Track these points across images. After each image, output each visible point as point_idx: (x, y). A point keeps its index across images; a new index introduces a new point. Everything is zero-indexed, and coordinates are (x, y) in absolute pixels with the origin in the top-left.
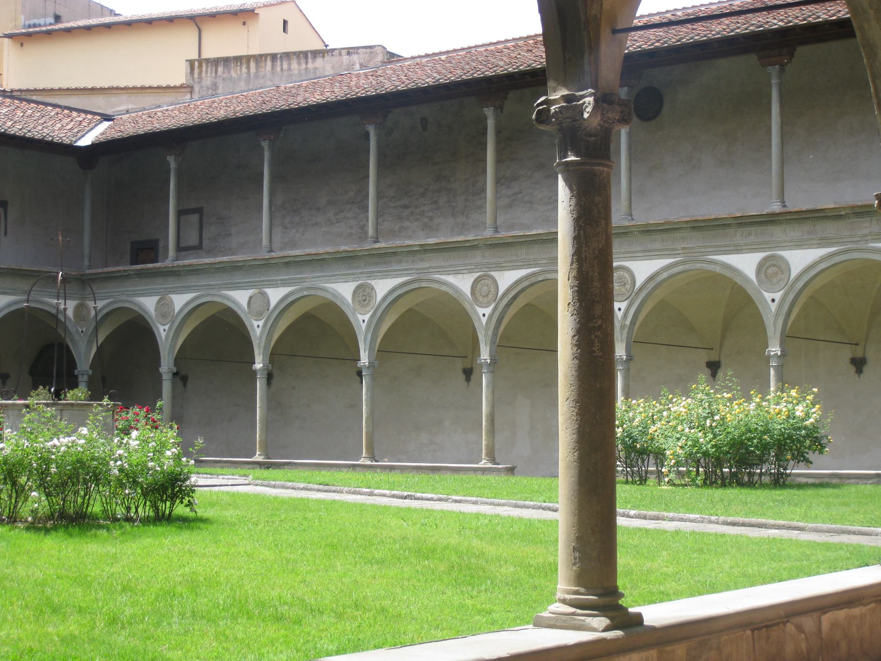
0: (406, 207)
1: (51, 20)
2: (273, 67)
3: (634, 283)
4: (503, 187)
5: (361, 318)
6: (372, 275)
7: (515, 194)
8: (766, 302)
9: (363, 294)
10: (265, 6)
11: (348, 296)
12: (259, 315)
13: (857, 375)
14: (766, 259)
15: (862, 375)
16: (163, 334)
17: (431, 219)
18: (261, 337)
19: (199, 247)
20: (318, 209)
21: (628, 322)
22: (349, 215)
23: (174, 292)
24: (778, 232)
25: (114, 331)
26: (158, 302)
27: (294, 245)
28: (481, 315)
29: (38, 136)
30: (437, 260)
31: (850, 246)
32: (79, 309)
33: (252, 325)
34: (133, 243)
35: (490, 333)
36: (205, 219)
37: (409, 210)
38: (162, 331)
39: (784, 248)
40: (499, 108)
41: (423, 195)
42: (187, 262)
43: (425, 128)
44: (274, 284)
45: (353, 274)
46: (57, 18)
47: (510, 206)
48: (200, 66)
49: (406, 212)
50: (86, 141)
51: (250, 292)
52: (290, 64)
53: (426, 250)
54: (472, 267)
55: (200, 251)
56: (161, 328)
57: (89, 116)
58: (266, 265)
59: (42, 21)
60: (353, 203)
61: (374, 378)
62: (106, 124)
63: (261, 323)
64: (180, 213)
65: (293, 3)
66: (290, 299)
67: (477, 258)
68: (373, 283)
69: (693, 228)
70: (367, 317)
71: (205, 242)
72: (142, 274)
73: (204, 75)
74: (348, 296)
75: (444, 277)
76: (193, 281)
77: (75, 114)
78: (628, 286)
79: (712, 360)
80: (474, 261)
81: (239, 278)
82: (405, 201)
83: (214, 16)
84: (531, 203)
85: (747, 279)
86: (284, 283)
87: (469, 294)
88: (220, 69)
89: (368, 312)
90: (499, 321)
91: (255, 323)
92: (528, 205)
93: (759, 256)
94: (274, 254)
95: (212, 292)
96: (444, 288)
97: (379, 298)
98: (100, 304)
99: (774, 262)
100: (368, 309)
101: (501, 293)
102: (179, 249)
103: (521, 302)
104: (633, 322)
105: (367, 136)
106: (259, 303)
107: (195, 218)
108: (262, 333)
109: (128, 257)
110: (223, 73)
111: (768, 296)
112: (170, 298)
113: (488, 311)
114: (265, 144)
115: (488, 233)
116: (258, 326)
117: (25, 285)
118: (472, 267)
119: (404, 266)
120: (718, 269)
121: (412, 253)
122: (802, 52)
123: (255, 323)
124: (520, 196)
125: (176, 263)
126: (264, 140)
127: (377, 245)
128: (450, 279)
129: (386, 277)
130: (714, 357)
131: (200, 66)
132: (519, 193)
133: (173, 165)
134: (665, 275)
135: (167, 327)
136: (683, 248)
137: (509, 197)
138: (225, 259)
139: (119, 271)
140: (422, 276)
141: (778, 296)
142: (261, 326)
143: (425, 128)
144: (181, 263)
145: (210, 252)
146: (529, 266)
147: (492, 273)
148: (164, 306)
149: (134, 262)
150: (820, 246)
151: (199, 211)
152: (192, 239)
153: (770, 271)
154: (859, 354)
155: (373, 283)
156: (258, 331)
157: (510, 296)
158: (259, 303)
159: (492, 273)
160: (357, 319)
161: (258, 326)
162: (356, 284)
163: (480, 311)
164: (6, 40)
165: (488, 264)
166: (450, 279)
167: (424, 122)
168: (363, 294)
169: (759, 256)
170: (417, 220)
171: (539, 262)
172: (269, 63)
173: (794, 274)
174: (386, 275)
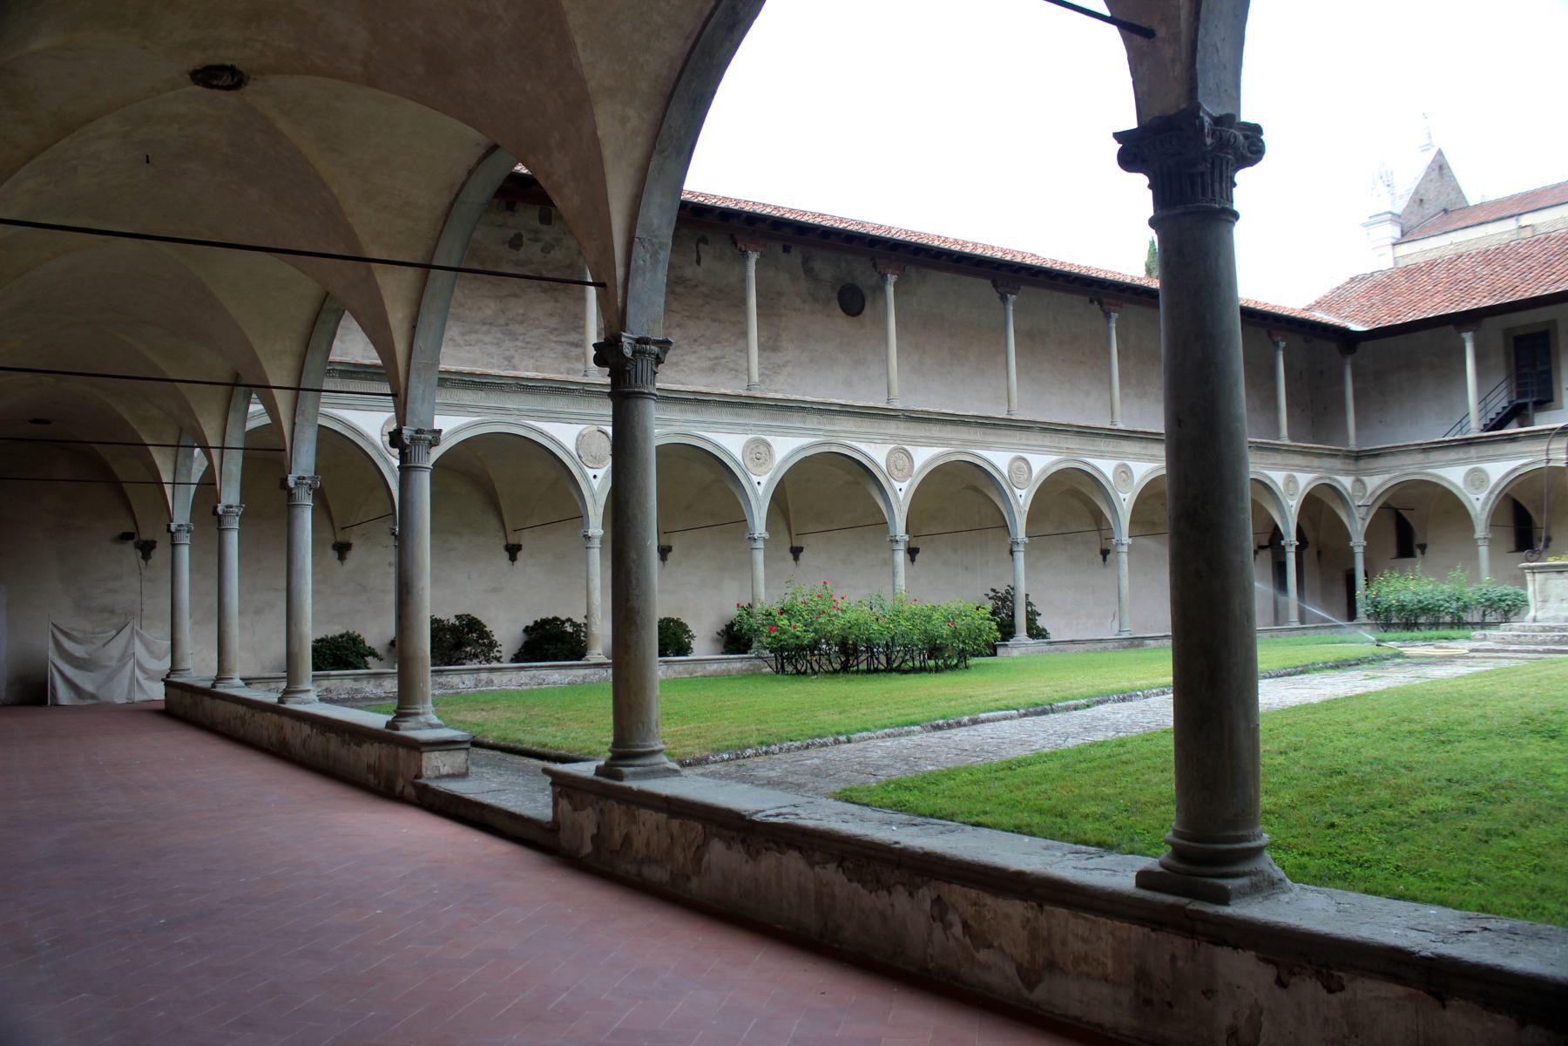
4: (703, 347)
7: (716, 358)
22: (487, 339)
28: (591, 477)
47: (713, 369)
54: (887, 437)
84: (737, 371)
89: (766, 473)
92: (734, 372)
100: (763, 469)
116: (595, 477)
118: (887, 437)
124: (724, 361)
128: (862, 446)
132: (723, 357)
137: (710, 359)
140: (834, 440)
142: (899, 492)
161: (595, 477)
168: (760, 451)
171: (953, 442)
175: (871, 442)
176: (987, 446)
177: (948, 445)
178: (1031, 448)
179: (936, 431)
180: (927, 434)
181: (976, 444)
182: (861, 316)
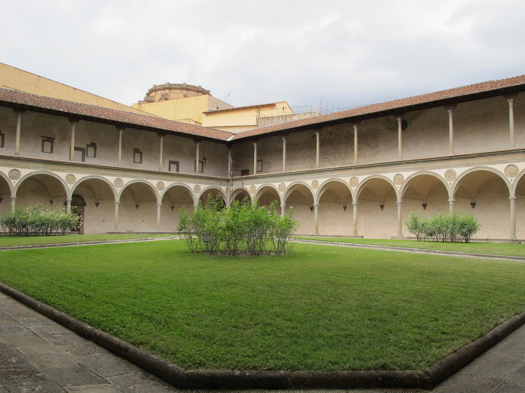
0: (325, 158)
1: (216, 109)
2: (282, 120)
3: (403, 179)
5: (314, 191)
6: (318, 177)
8: (448, 184)
9: (315, 183)
10: (278, 103)
11: (310, 185)
12: (282, 190)
13: (473, 208)
14: (448, 171)
15: (474, 208)
16: (253, 196)
17: (333, 161)
18: (283, 196)
19: (261, 171)
20: (298, 159)
21: (401, 191)
23: (256, 184)
24: (452, 162)
25: (237, 195)
26: (251, 186)
27: (291, 170)
29: (215, 138)
30: (339, 173)
31: (477, 166)
32: (227, 189)
33: (280, 193)
34: (242, 171)
35: (356, 195)
36: (263, 163)
37: (326, 159)
38: (253, 195)
39: (454, 167)
40: (358, 126)
41: (331, 154)
42: (260, 175)
43: (331, 135)
44: (287, 181)
45: (312, 177)
46: (218, 108)
48: (260, 120)
49: (325, 160)
50: (229, 139)
51: (279, 184)
52: (287, 118)
53: (335, 170)
55: (262, 172)
56: (252, 194)
57: (229, 134)
58: (285, 175)
59: (213, 109)
60: (309, 157)
61: (319, 208)
62: (234, 136)
63: (283, 192)
64: (258, 161)
65: (285, 103)
66: (292, 185)
67: (352, 172)
68: (318, 180)
69: (423, 161)
70: (316, 190)
71: (263, 170)
72: (246, 178)
73: (261, 122)
74: (310, 185)
75: (341, 178)
76: (262, 180)
77: (225, 133)
78: (401, 180)
79: (424, 204)
80: (351, 173)
81: (276, 179)
82: (325, 156)
83: (263, 106)
84: (365, 156)
85: (442, 178)
86: (290, 180)
87: (349, 183)
88: (266, 120)
90: (359, 191)
91: (281, 193)
93: (445, 170)
94: (287, 172)
95: (268, 183)
96: (341, 181)
97: (320, 184)
98: (234, 187)
99: (451, 172)
101: (359, 183)
102: (257, 172)
103: (365, 186)
104: (403, 191)
105: (314, 137)
106: (282, 186)
107: (260, 163)
108: (283, 195)
109: (240, 174)
110: (267, 121)
111: (449, 183)
112: (255, 186)
113: (355, 188)
114: (284, 139)
115: (355, 164)
117: (211, 182)
119: (328, 175)
120: (431, 174)
121: (330, 170)
122: (459, 105)
123: (281, 193)
125: (257, 175)
126: (284, 138)
127: (319, 169)
128: (343, 178)
129: (322, 178)
130: (425, 203)
131: (260, 120)
132: (361, 153)
133: (255, 146)
134: (414, 176)
135: (254, 194)
136: (420, 168)
138: (272, 173)
139: (239, 178)
140: (334, 178)
141: (452, 182)
143: (331, 135)
144: (258, 175)
145: (264, 173)
146: (369, 174)
147: (356, 176)
148: (253, 187)
149: (242, 174)
150: (467, 166)
151: (262, 161)
152: (260, 170)
153: (449, 174)
154: (473, 201)
155: (318, 180)
156: (282, 195)
157: (362, 183)
158: (282, 186)
159: (356, 176)
160: (313, 191)
162: (313, 180)
163: (353, 188)
164: (204, 114)
165: (355, 173)
166: (343, 178)
167: (331, 133)
168: (315, 183)
169: (445, 170)
170: (329, 162)
172: (281, 118)
173: (457, 176)
174: (322, 177)
175: (345, 177)
176: (385, 172)
177: (372, 174)
178: (403, 170)
179: (367, 170)
180: (364, 172)
181: (381, 172)
182: (406, 130)
